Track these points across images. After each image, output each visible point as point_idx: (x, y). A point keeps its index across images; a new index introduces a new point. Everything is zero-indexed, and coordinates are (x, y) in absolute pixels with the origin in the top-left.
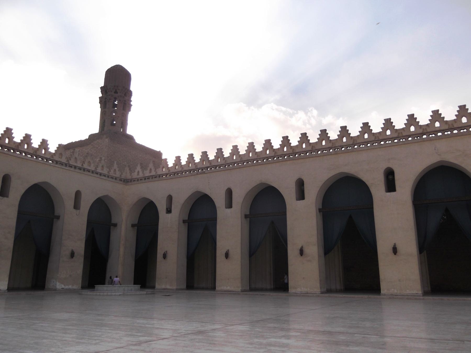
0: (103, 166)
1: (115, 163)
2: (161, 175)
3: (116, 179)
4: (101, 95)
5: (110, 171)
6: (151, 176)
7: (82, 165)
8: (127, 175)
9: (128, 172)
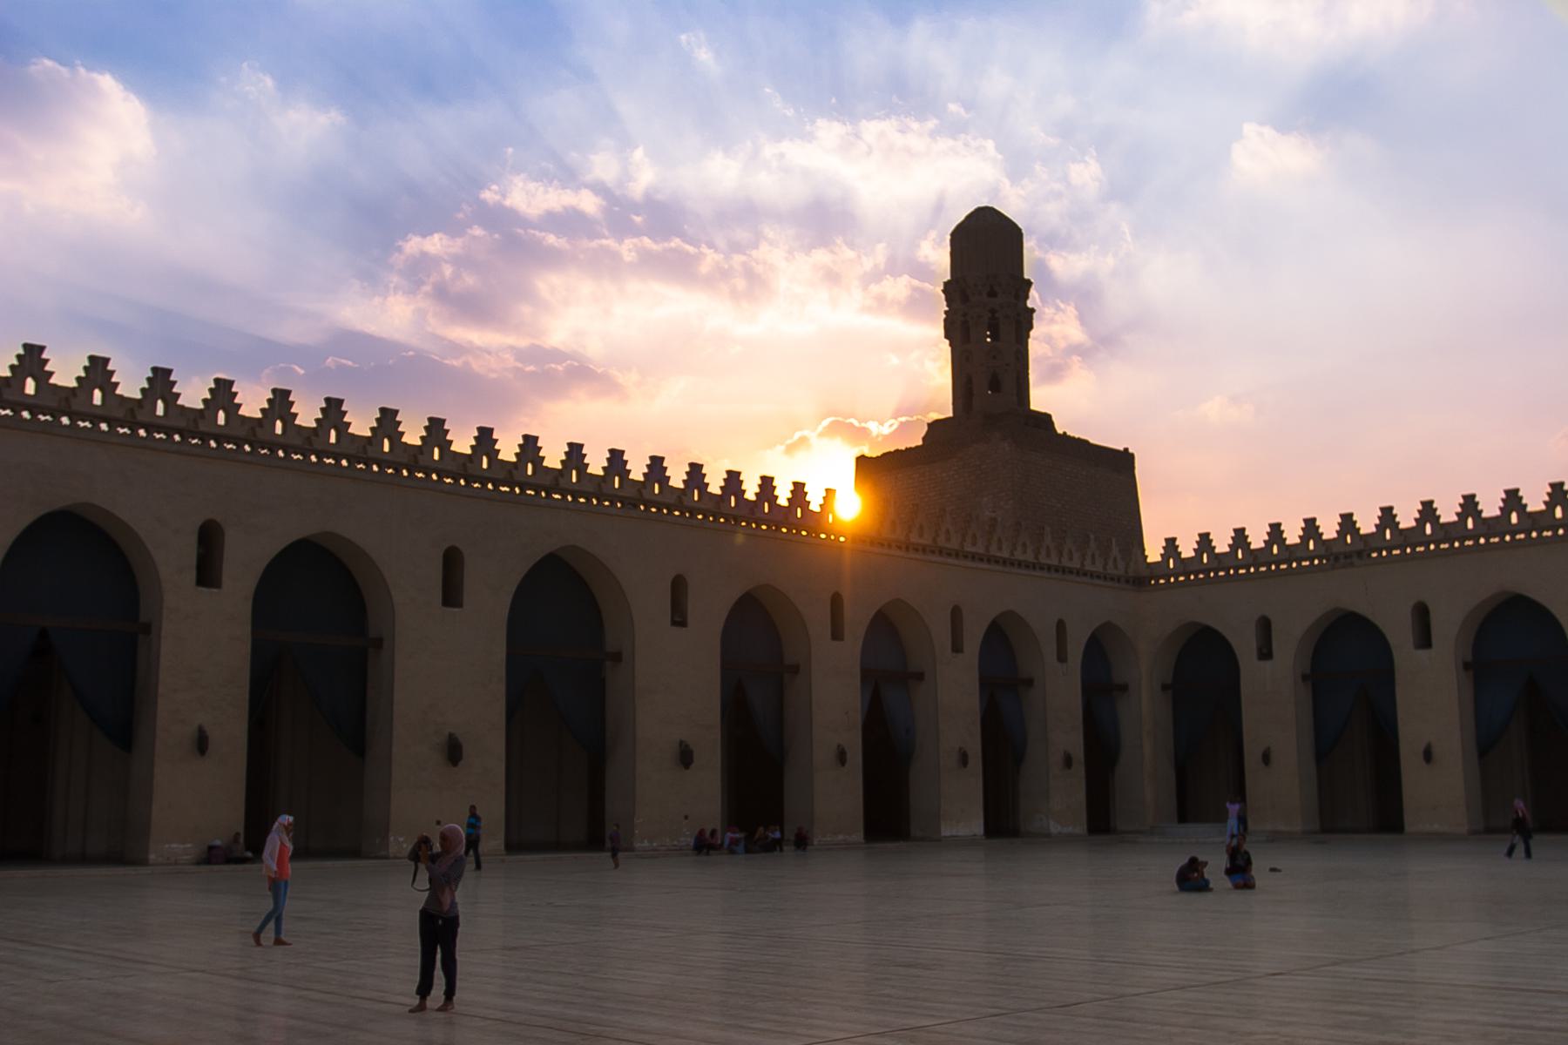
0: (1093, 556)
1: (1114, 543)
3: (1119, 581)
7: (1060, 561)
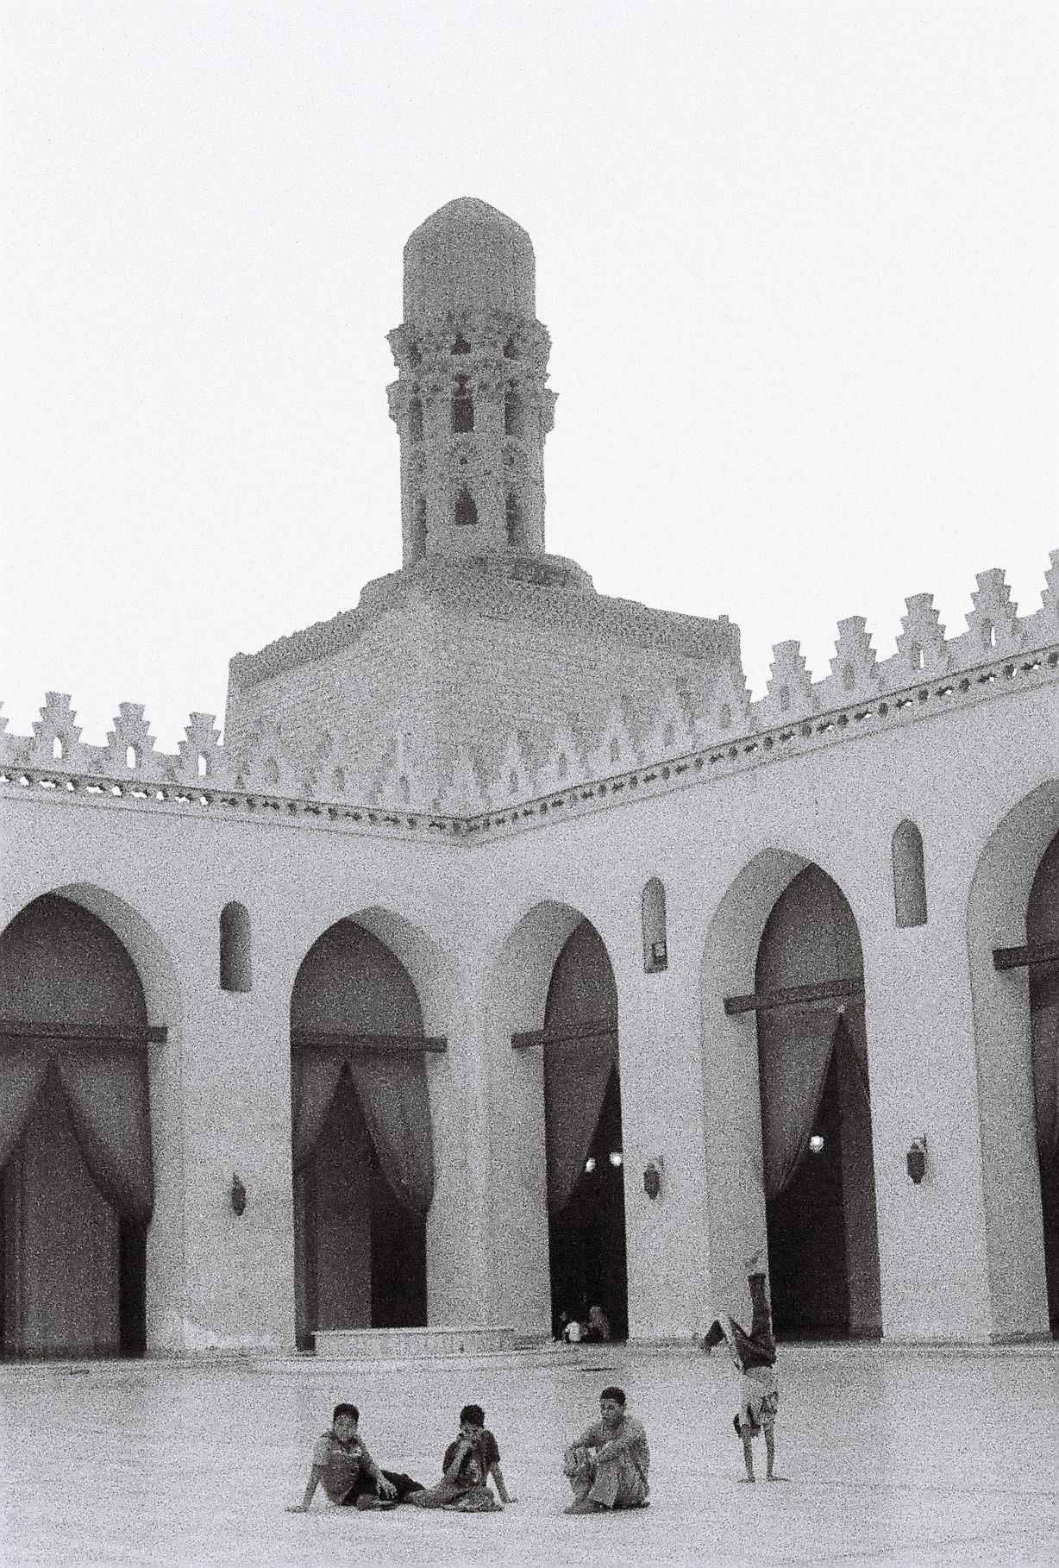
2: (607, 785)
4: (393, 374)
5: (380, 791)
6: (564, 792)
8: (465, 798)
9: (472, 777)
